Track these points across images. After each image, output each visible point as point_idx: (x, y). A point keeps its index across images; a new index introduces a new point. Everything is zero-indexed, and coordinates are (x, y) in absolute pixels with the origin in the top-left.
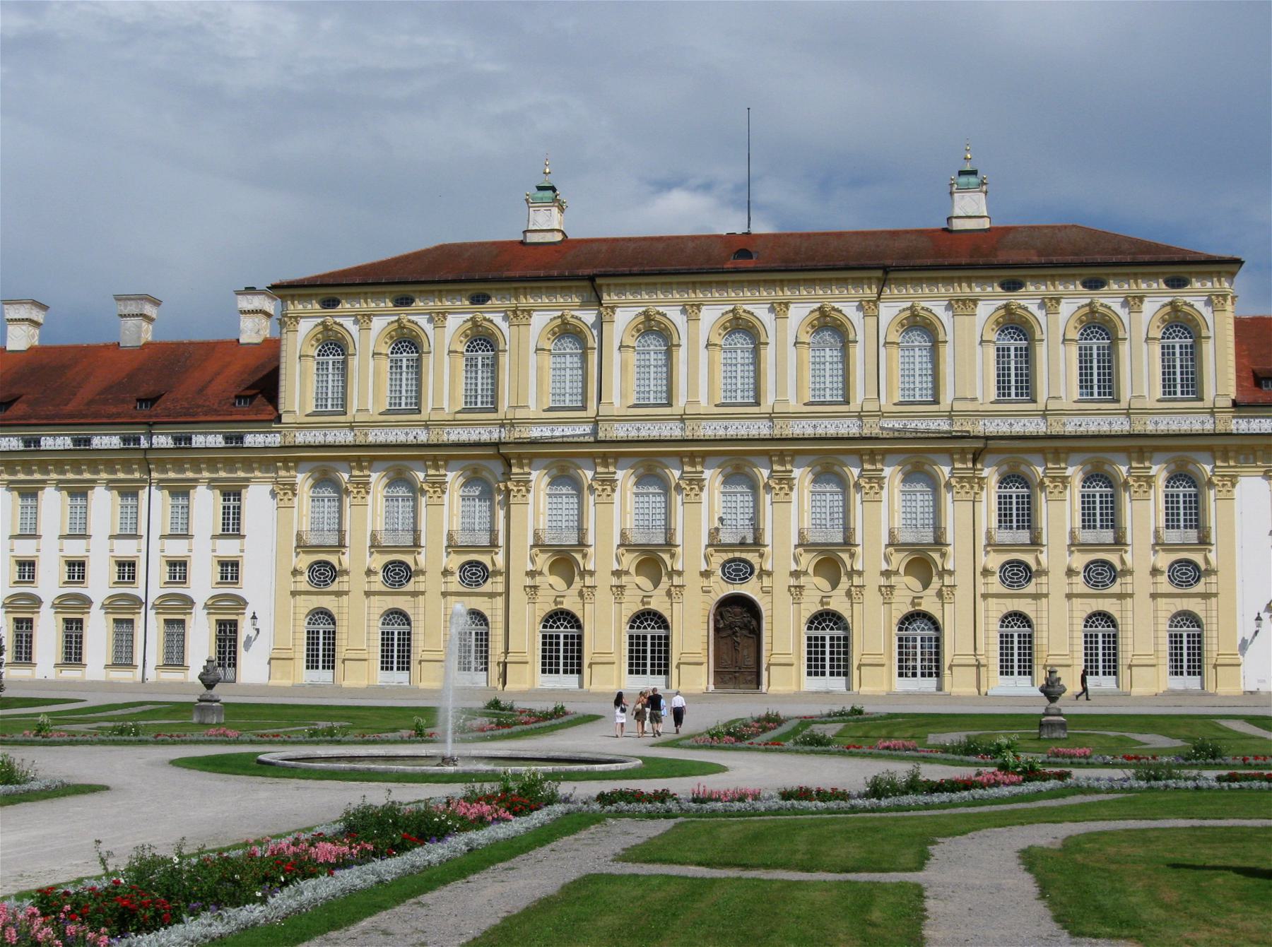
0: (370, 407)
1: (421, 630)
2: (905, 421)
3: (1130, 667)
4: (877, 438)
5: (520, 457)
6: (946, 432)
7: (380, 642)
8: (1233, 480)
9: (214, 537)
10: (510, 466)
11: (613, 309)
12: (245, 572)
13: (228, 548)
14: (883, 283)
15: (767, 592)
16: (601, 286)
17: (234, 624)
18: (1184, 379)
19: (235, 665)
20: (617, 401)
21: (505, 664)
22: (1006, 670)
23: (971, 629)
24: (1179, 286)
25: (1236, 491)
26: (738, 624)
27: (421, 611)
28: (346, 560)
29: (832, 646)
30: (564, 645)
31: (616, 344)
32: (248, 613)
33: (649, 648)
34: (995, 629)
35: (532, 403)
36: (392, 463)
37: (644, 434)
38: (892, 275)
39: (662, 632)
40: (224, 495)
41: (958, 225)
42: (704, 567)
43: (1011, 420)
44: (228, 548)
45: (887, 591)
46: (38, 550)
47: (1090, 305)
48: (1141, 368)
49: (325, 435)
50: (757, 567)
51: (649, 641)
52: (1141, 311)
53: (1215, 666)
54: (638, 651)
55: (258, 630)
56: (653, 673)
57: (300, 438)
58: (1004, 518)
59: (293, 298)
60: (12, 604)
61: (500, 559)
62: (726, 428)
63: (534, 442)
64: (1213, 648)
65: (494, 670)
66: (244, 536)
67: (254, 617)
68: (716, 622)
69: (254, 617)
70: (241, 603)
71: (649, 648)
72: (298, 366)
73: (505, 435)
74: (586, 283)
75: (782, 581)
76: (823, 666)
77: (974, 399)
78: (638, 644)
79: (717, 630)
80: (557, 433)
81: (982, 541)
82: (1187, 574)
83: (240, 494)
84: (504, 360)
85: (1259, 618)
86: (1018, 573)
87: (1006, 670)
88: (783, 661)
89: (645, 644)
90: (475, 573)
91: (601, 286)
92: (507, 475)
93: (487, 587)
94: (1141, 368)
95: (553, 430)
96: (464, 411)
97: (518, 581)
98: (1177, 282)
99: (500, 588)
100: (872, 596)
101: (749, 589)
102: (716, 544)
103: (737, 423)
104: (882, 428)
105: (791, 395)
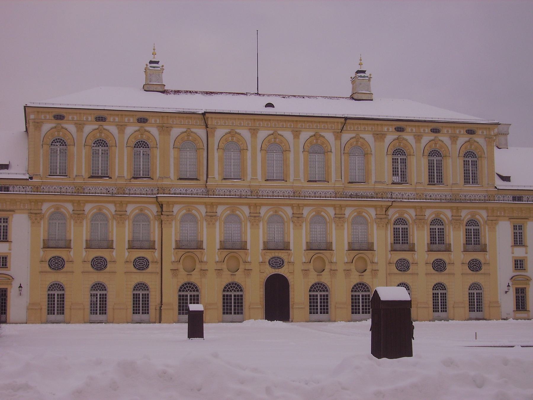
0: (83, 174)
7: (47, 299)
10: (162, 208)
11: (214, 128)
16: (208, 118)
19: (5, 313)
20: (216, 176)
21: (161, 310)
25: (497, 227)
29: (235, 299)
31: (216, 147)
33: (233, 301)
35: (172, 175)
38: (348, 121)
39: (61, 292)
42: (261, 260)
45: (347, 272)
46: (10, 250)
50: (286, 261)
53: (489, 307)
56: (235, 313)
58: (396, 240)
61: (157, 254)
64: (487, 298)
67: (20, 287)
69: (20, 287)
72: (41, 151)
78: (227, 299)
81: (389, 248)
82: (475, 266)
84: (157, 153)
85: (509, 286)
89: (231, 299)
91: (208, 118)
97: (167, 267)
99: (159, 270)
101: (282, 271)
102: (267, 248)
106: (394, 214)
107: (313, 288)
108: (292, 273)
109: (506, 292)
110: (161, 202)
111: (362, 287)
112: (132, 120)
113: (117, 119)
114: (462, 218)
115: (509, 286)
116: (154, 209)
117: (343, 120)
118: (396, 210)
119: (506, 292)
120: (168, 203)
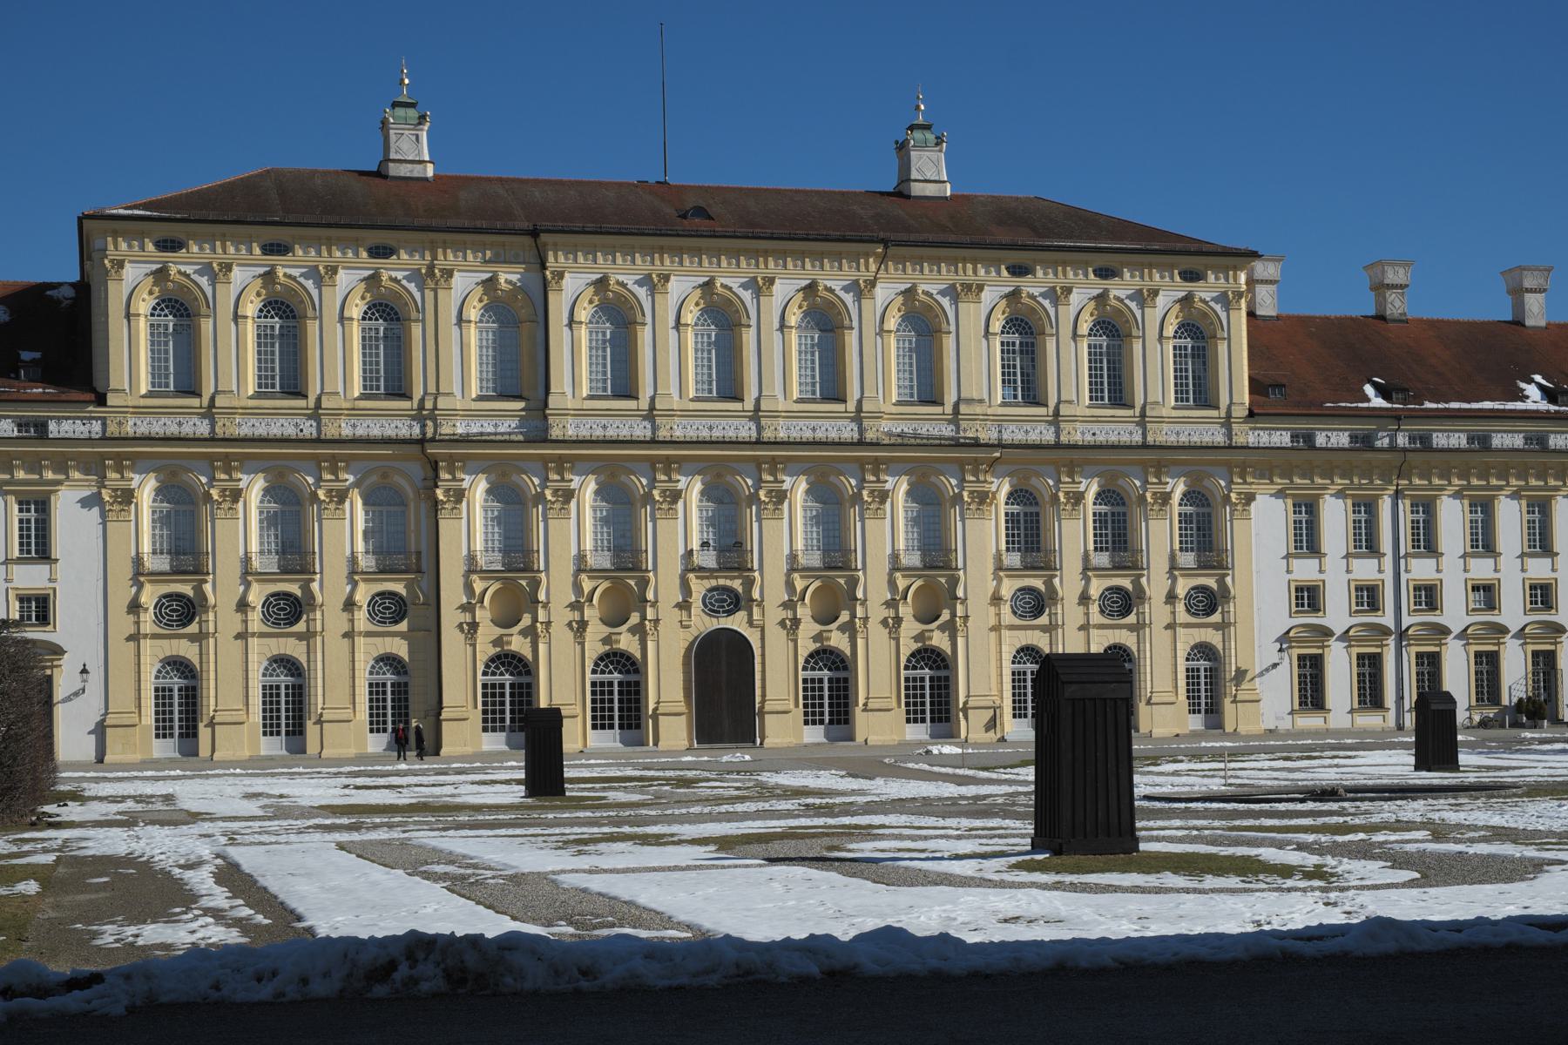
2: (915, 424)
4: (878, 444)
5: (451, 459)
6: (951, 439)
8: (1250, 498)
10: (436, 469)
12: (61, 611)
14: (883, 260)
16: (545, 245)
18: (1199, 388)
20: (568, 390)
24: (1191, 280)
37: (611, 433)
38: (893, 250)
40: (20, 503)
41: (917, 189)
43: (1028, 426)
48: (1155, 367)
49: (180, 424)
52: (1159, 304)
57: (133, 426)
59: (115, 234)
62: (711, 428)
63: (466, 440)
67: (84, 671)
69: (84, 671)
74: (527, 240)
75: (774, 614)
76: (611, 718)
77: (981, 401)
78: (602, 693)
80: (501, 429)
88: (779, 708)
91: (545, 245)
92: (435, 481)
94: (1155, 367)
95: (496, 426)
98: (1191, 276)
103: (724, 422)
104: (890, 434)
109: (1275, 665)
115: (1281, 650)
116: (417, 470)
119: (1275, 665)
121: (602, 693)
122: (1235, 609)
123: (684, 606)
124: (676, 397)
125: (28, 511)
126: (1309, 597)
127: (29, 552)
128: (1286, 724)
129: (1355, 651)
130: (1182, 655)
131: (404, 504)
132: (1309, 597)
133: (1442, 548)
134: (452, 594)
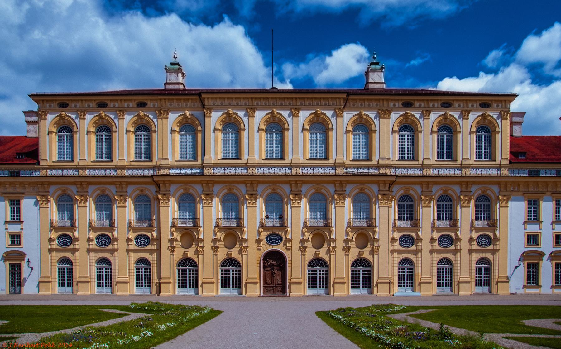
1: (117, 268)
3: (459, 283)
9: (6, 222)
13: (14, 228)
15: (289, 249)
17: (19, 266)
22: (401, 285)
23: (385, 265)
26: (275, 264)
27: (116, 258)
28: (76, 234)
30: (189, 274)
32: (26, 260)
33: (231, 276)
34: (396, 266)
36: (99, 186)
44: (14, 228)
45: (347, 249)
47: (444, 114)
50: (284, 237)
51: (231, 272)
54: (225, 277)
55: (32, 268)
60: (7, 257)
64: (497, 274)
65: (154, 288)
66: (23, 222)
68: (264, 263)
70: (22, 255)
71: (231, 276)
73: (158, 172)
75: (296, 245)
78: (225, 274)
79: (264, 267)
82: (486, 241)
83: (19, 201)
86: (408, 241)
87: (401, 285)
89: (229, 274)
90: (143, 240)
93: (149, 247)
96: (136, 161)
100: (339, 251)
101: (280, 248)
105: (300, 155)
106: (399, 190)
107: (312, 263)
108: (289, 249)
110: (157, 181)
111: (319, 262)
112: (131, 105)
113: (117, 105)
114: (472, 193)
117: (344, 96)
118: (402, 186)
119: (516, 267)
120: (164, 183)
121: (225, 274)
122: (499, 245)
123: (258, 241)
124: (257, 158)
125: (14, 204)
126: (533, 239)
127: (14, 219)
128: (521, 291)
129: (554, 262)
130: (435, 263)
131: (150, 201)
132: (533, 239)
133: (542, 219)
134: (166, 236)
